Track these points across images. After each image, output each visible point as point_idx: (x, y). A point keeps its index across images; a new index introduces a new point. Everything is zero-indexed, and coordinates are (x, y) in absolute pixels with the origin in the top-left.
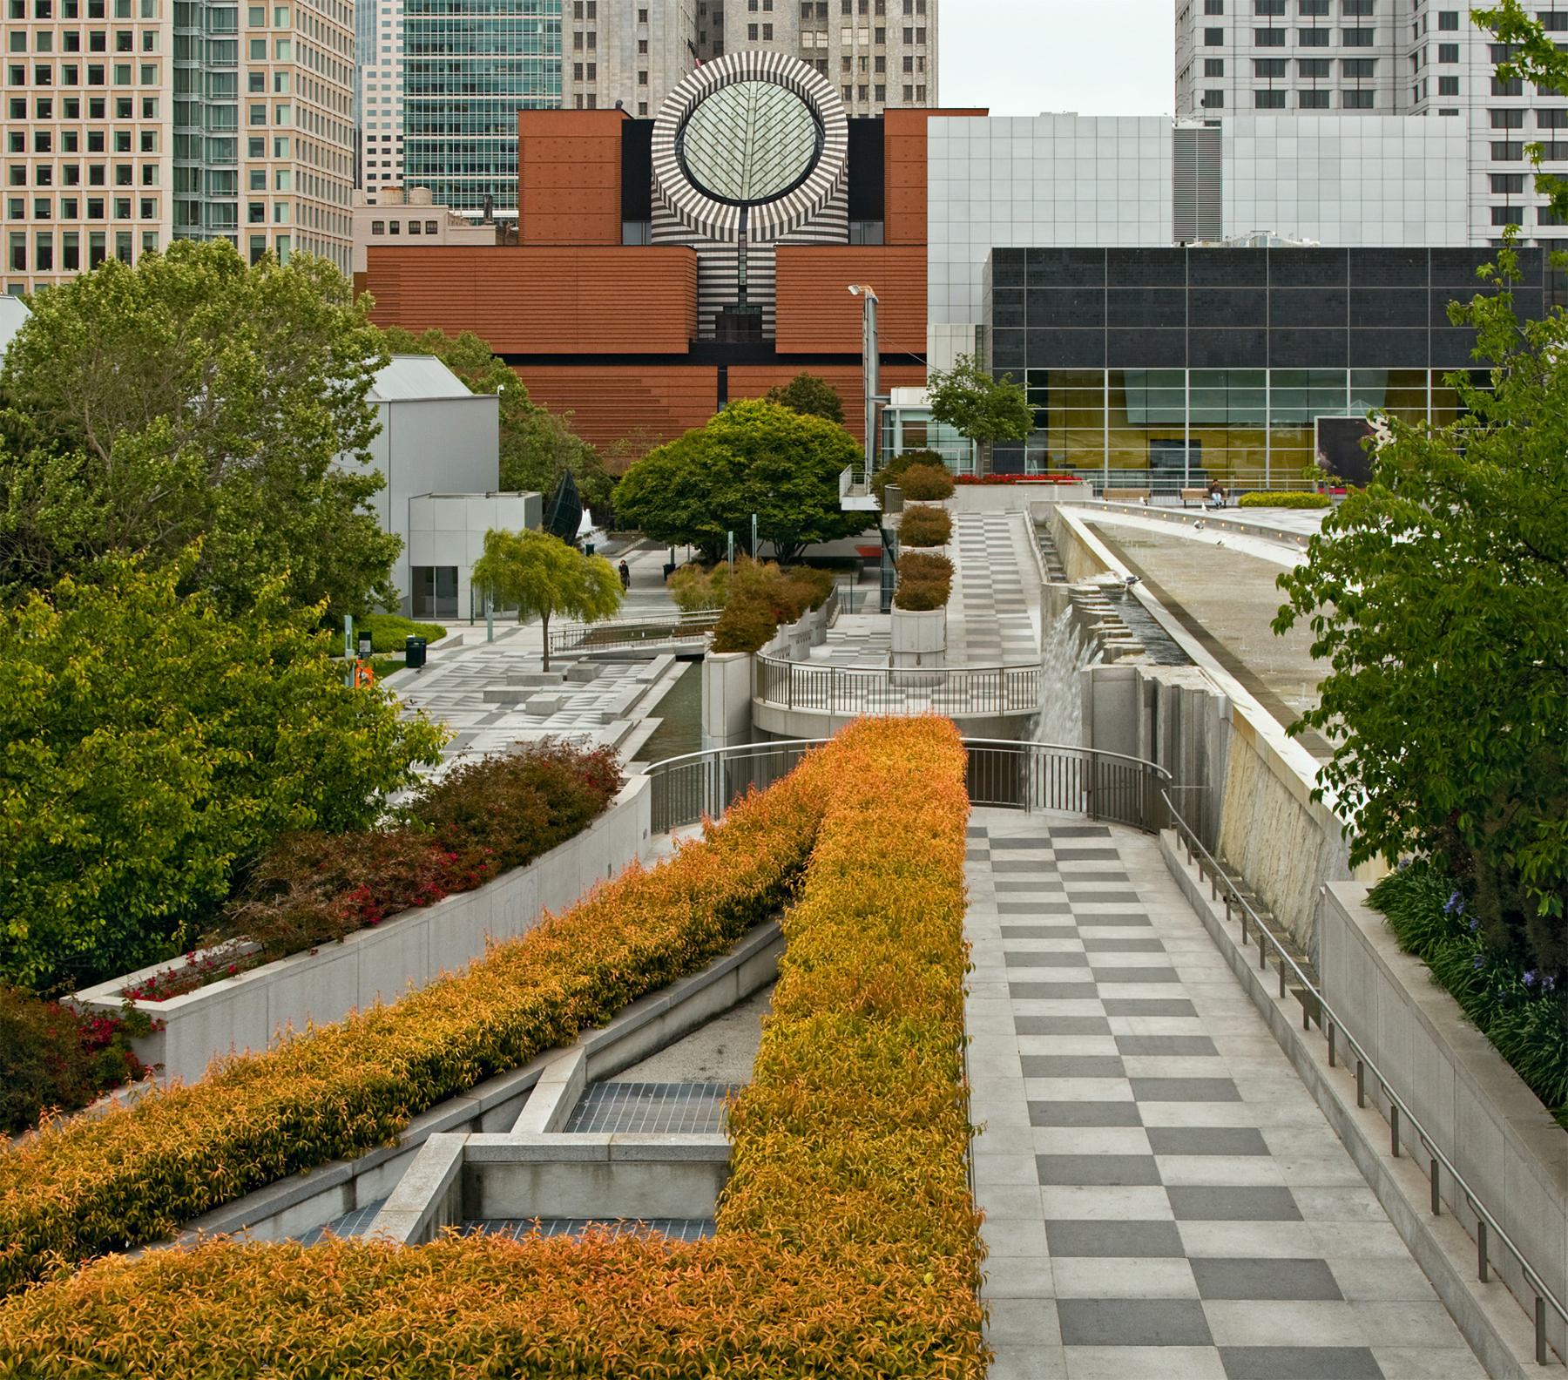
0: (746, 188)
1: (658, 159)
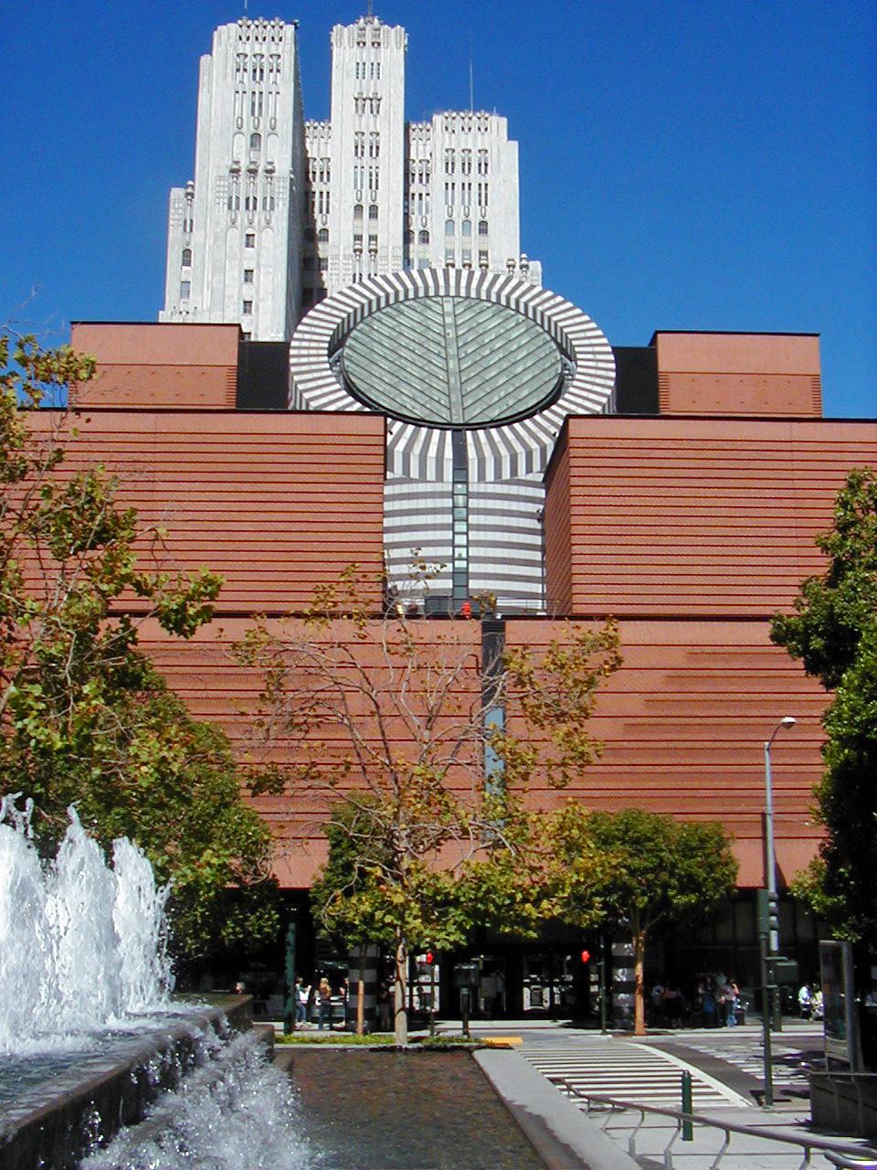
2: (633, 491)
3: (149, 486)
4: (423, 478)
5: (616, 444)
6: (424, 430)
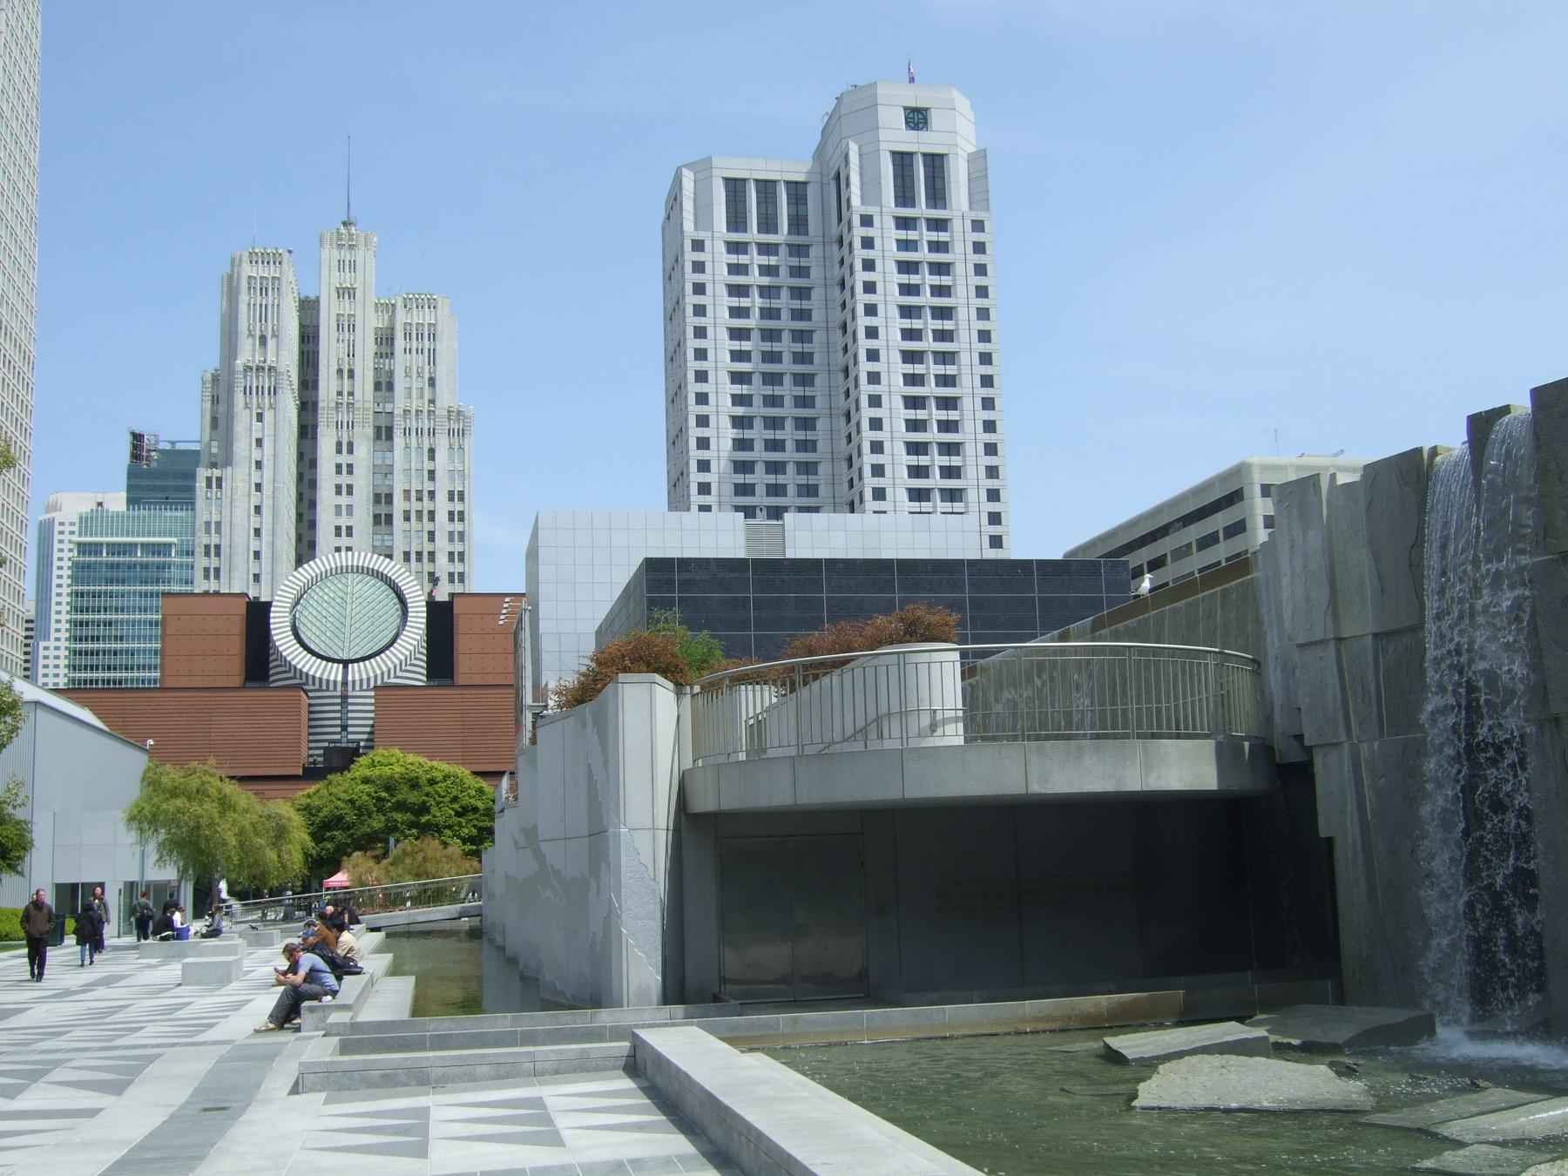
0: (346, 650)
1: (275, 629)
4: (328, 690)
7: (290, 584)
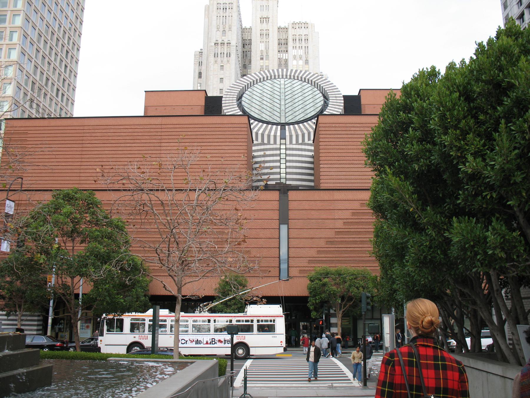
2: (344, 143)
3: (159, 145)
4: (269, 143)
5: (337, 125)
6: (270, 126)
7: (238, 84)
